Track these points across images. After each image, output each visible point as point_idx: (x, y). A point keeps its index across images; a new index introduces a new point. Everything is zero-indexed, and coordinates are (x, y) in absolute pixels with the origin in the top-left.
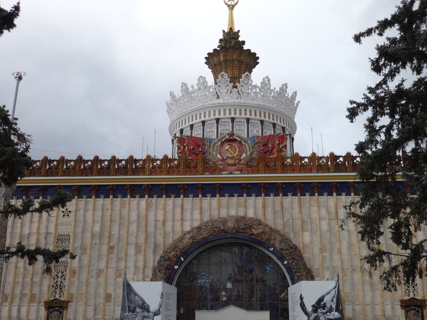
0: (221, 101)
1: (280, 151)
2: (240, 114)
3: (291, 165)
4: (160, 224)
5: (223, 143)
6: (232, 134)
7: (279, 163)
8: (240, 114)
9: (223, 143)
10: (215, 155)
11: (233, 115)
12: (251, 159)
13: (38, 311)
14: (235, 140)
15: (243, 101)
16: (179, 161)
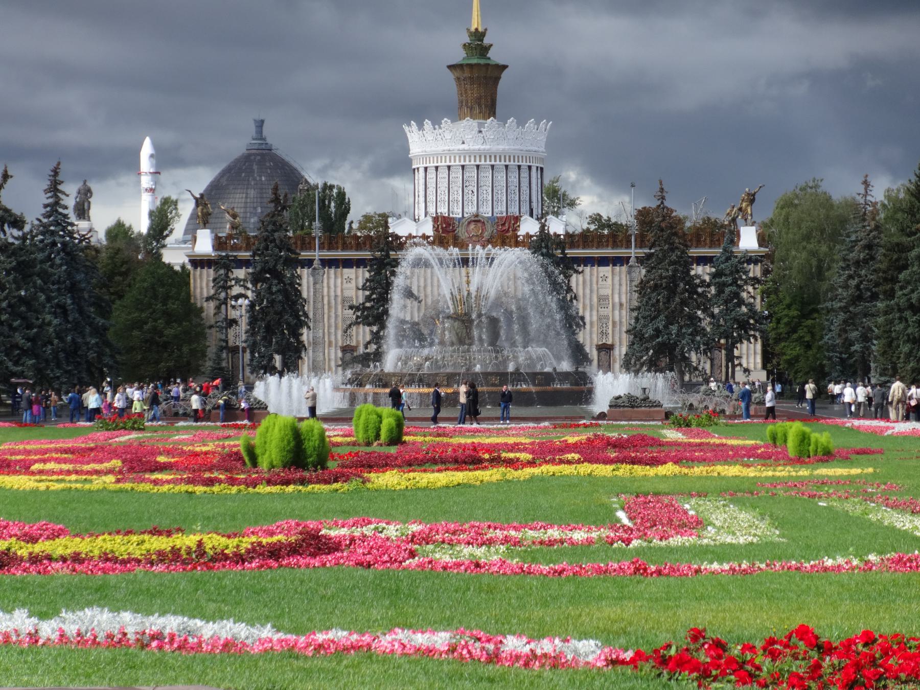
0: (465, 147)
1: (515, 230)
2: (485, 161)
3: (523, 242)
4: (422, 289)
5: (469, 223)
6: (477, 216)
7: (512, 240)
8: (485, 161)
9: (469, 223)
10: (462, 233)
11: (478, 163)
12: (492, 237)
13: (336, 353)
14: (479, 221)
15: (487, 147)
16: (434, 237)
